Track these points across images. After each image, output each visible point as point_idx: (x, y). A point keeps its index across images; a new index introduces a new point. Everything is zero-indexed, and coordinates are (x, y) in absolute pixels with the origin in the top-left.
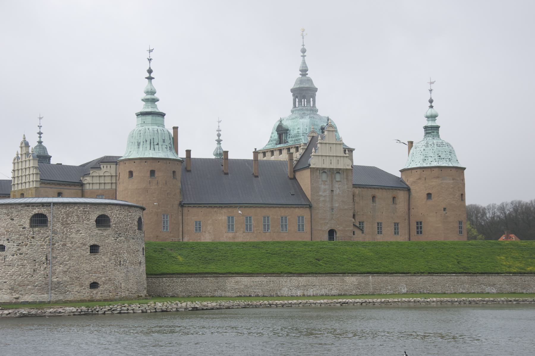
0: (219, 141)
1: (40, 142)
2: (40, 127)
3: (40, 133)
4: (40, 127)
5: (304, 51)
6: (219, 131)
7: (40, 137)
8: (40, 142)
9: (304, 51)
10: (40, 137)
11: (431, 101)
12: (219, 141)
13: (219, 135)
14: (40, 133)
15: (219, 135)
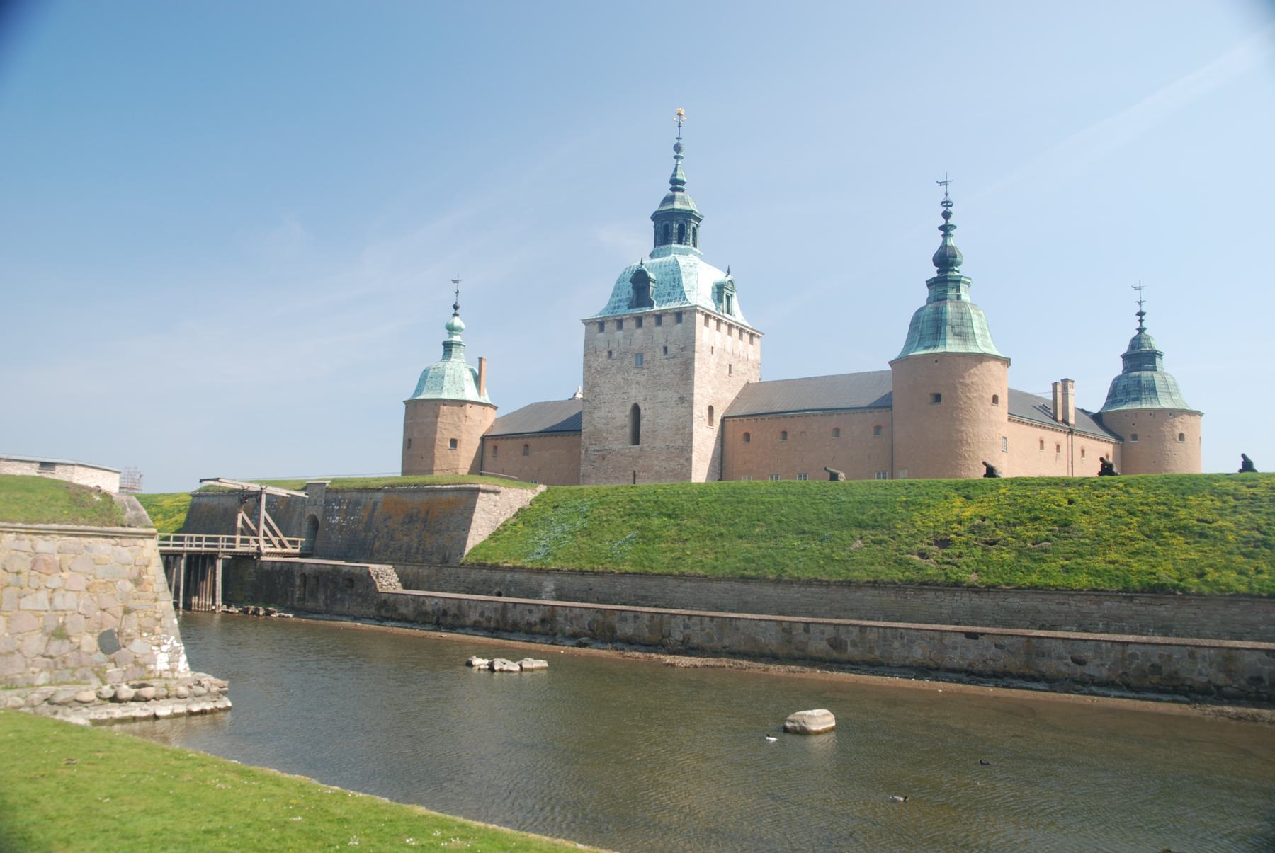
0: (946, 230)
1: (1141, 330)
2: (1140, 303)
3: (1141, 314)
4: (1140, 303)
5: (677, 148)
6: (947, 204)
7: (1141, 321)
8: (1141, 330)
9: (677, 148)
10: (1141, 321)
11: (456, 307)
12: (946, 230)
13: (946, 215)
14: (1141, 314)
15: (946, 215)
